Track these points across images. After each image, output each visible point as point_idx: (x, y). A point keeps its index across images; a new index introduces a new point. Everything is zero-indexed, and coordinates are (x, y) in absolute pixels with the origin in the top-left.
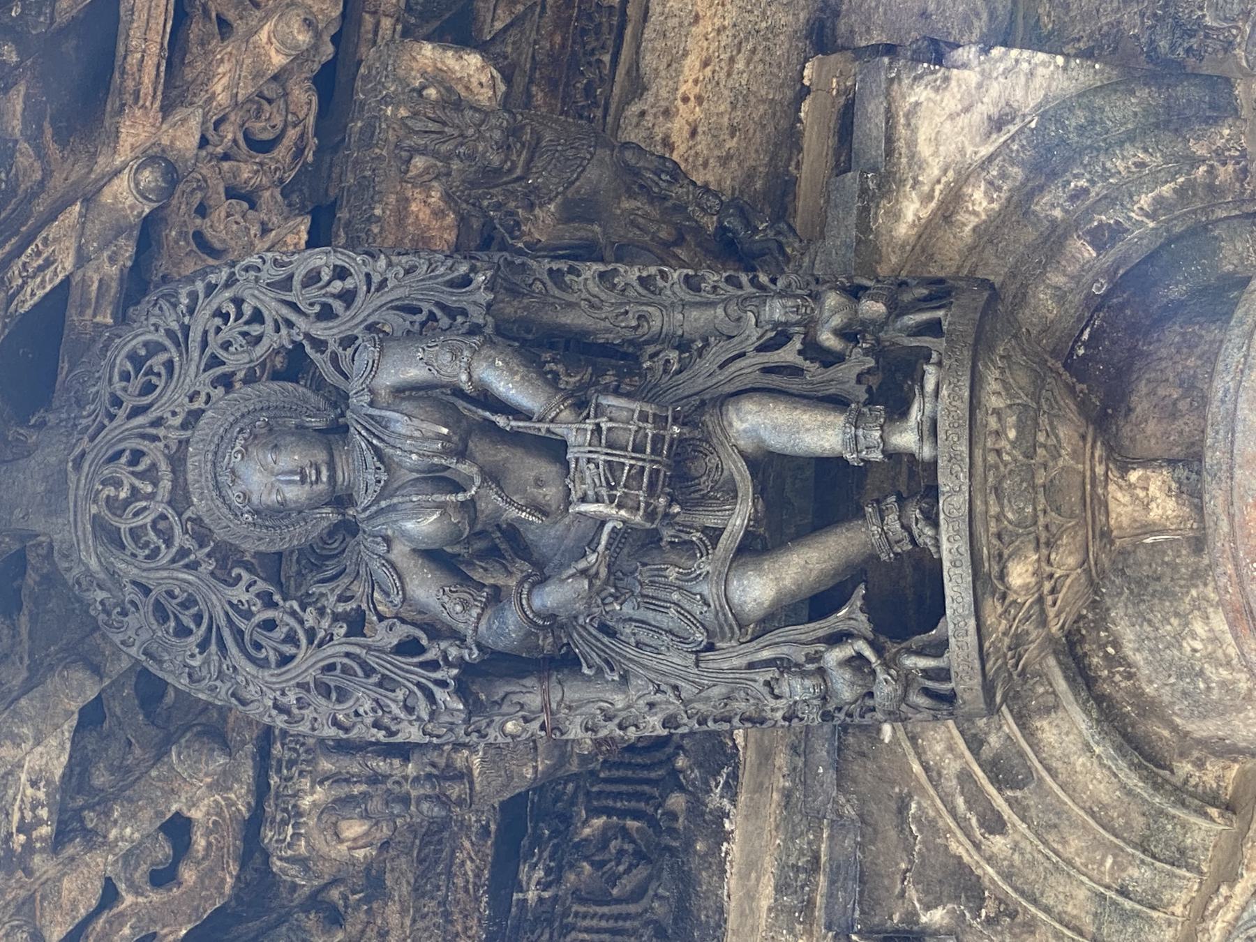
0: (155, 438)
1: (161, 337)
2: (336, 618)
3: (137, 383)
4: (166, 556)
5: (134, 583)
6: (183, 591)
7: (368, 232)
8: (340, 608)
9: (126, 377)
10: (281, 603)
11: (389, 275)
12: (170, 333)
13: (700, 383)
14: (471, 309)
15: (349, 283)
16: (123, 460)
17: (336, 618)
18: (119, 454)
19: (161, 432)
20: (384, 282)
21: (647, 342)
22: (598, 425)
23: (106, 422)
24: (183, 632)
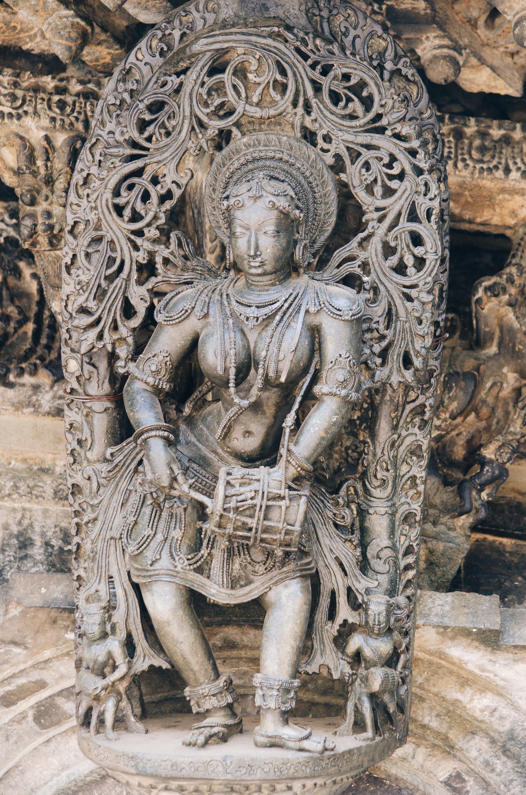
0: (295, 104)
1: (376, 109)
2: (151, 254)
3: (340, 88)
4: (202, 113)
5: (181, 84)
6: (174, 128)
7: (496, 167)
8: (159, 260)
9: (346, 77)
10: (163, 209)
11: (416, 303)
12: (379, 117)
13: (325, 541)
14: (386, 371)
15: (411, 270)
16: (279, 77)
17: (151, 254)
18: (283, 72)
19: (300, 110)
20: (409, 299)
21: (364, 485)
22: (283, 498)
23: (310, 62)
24: (143, 125)
